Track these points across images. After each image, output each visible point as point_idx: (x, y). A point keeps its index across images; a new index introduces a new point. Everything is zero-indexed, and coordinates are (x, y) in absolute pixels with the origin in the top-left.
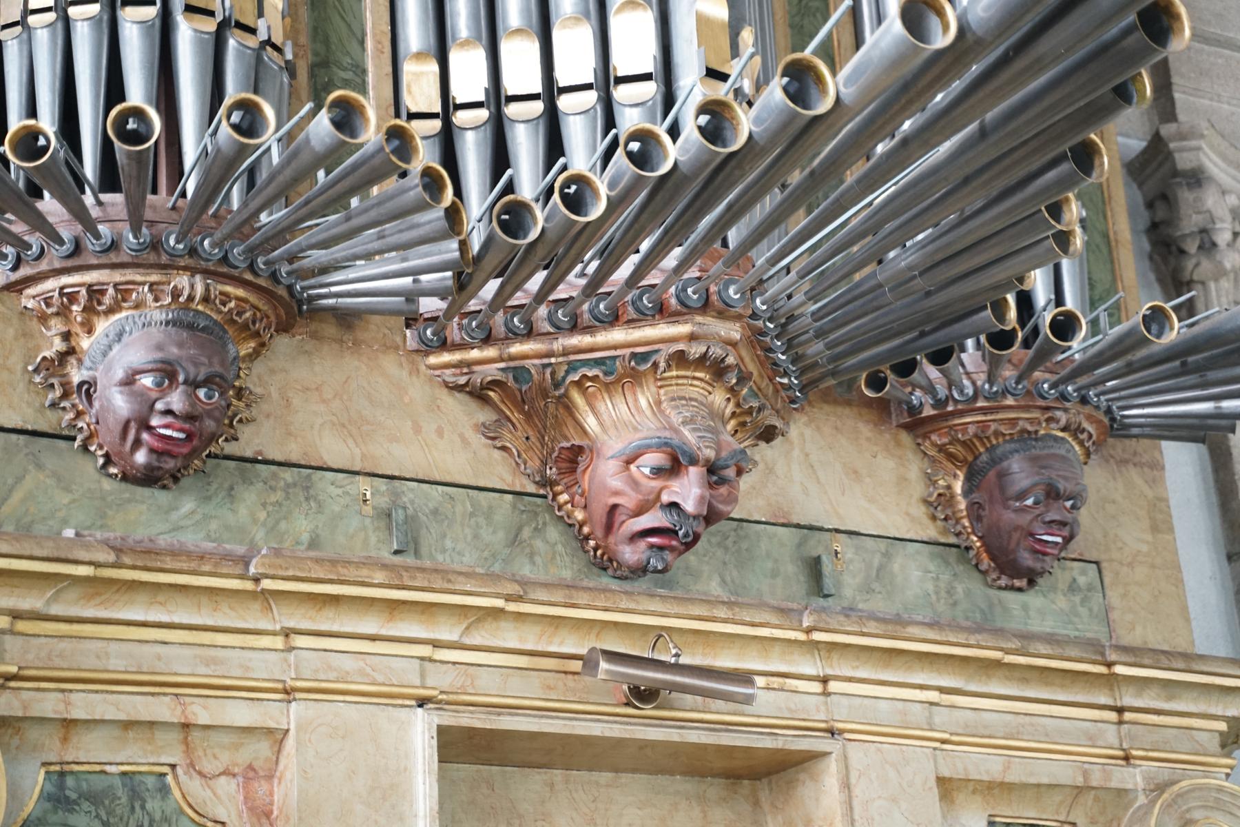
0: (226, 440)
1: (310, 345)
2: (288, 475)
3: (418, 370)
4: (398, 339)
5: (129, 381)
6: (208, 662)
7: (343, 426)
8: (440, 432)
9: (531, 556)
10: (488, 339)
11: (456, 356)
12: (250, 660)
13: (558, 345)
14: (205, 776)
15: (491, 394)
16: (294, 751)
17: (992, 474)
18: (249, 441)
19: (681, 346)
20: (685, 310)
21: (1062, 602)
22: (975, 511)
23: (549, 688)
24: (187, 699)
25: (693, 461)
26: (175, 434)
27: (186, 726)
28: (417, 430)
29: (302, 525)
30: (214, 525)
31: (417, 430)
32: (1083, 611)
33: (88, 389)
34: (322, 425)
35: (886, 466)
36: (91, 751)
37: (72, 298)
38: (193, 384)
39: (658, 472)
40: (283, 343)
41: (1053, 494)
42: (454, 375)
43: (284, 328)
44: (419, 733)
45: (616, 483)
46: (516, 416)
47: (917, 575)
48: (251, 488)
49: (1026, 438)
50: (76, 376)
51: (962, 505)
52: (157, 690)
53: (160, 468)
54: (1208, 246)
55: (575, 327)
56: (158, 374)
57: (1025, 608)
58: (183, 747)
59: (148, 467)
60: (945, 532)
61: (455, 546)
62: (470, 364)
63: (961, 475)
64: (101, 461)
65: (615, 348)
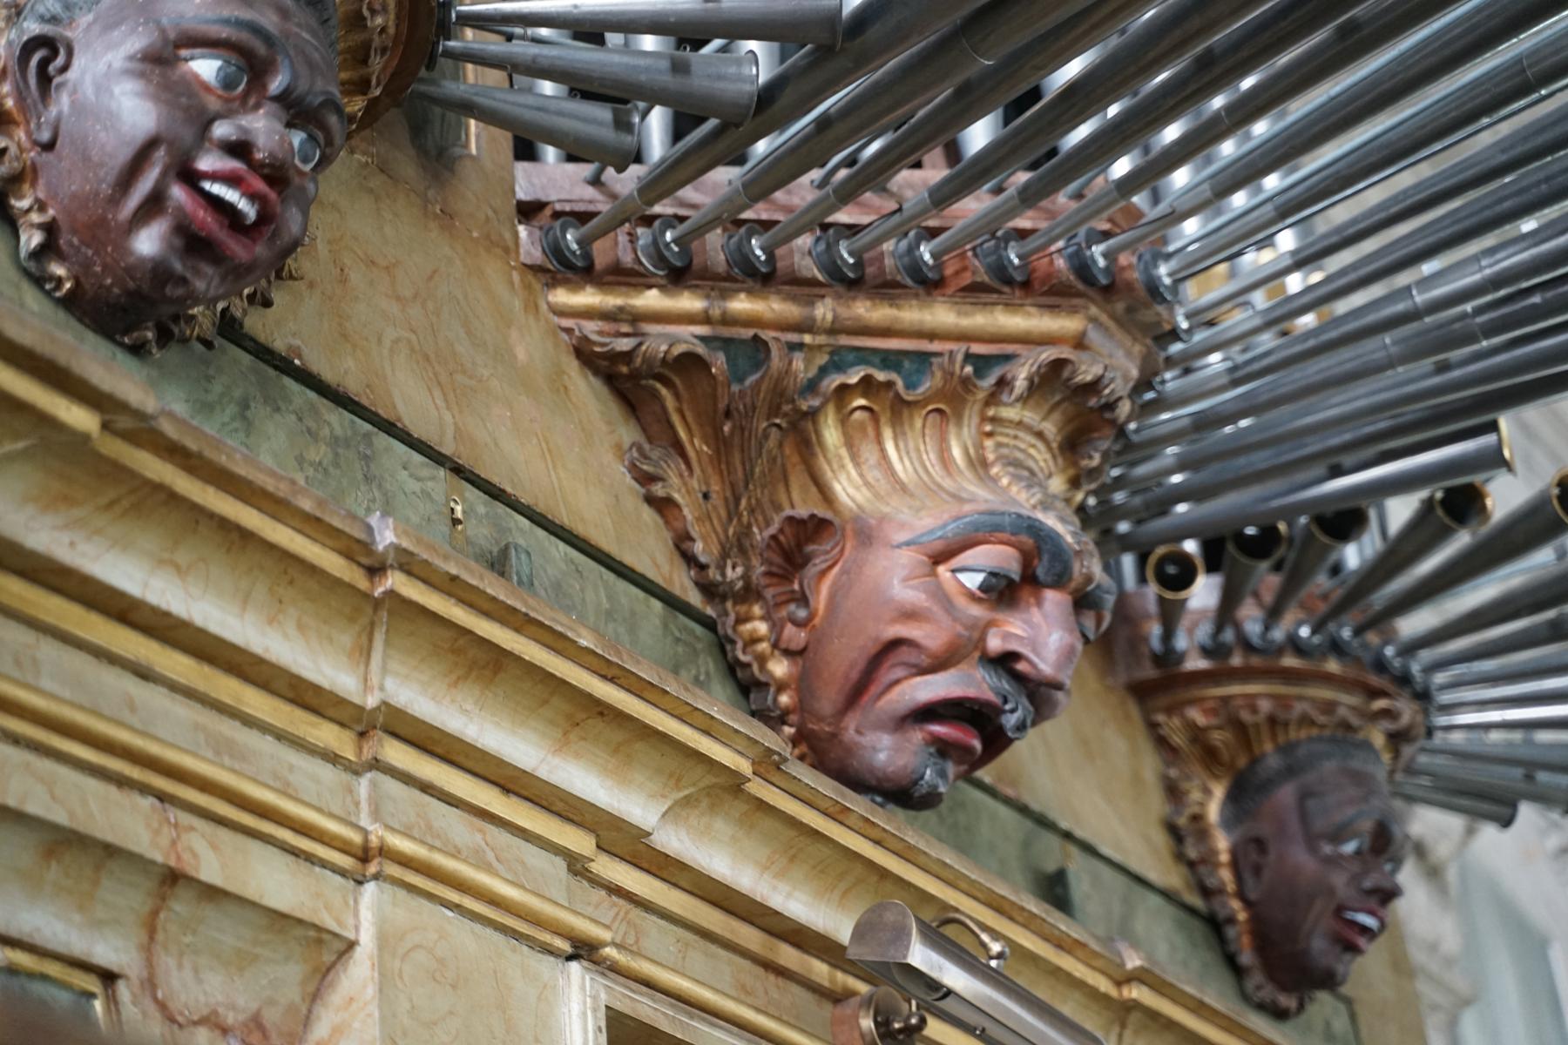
0: (251, 298)
1: (377, 181)
2: (337, 419)
3: (537, 307)
4: (508, 235)
7: (427, 358)
11: (612, 301)
12: (291, 768)
13: (824, 311)
14: (172, 1020)
15: (664, 391)
16: (371, 991)
17: (1286, 794)
18: (287, 323)
19: (1065, 352)
20: (1054, 295)
23: (743, 988)
24: (186, 818)
25: (1059, 582)
26: (243, 205)
27: (173, 878)
34: (396, 341)
42: (600, 333)
45: (907, 593)
46: (697, 446)
48: (277, 416)
51: (1222, 843)
52: (134, 772)
53: (183, 281)
56: (234, 58)
58: (143, 937)
59: (159, 272)
62: (637, 318)
63: (1219, 791)
64: (32, 239)
65: (932, 336)
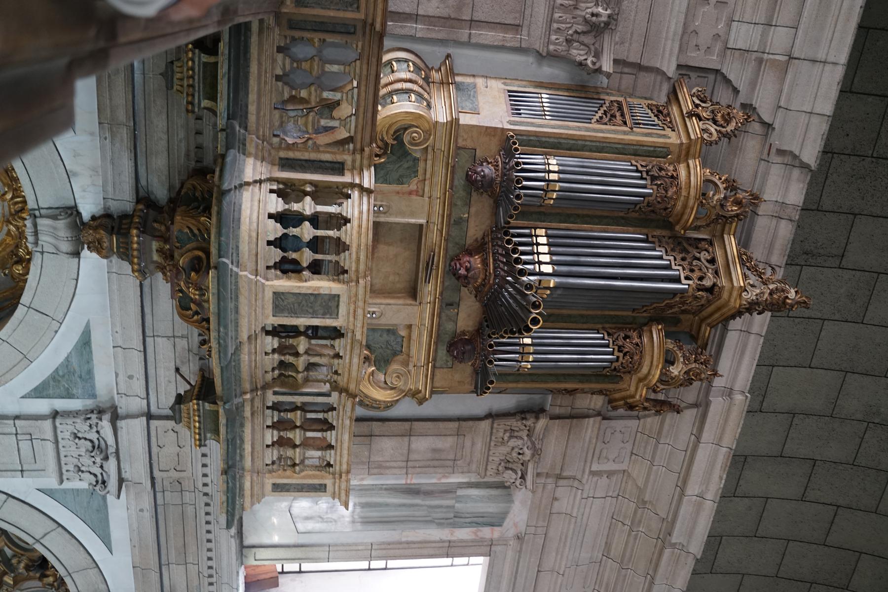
5: (483, 171)
18: (474, 194)
21: (444, 358)
22: (461, 339)
33: (482, 165)
35: (471, 323)
36: (421, 165)
40: (491, 201)
41: (464, 353)
44: (423, 221)
47: (449, 326)
49: (474, 349)
54: (523, 419)
55: (493, 253)
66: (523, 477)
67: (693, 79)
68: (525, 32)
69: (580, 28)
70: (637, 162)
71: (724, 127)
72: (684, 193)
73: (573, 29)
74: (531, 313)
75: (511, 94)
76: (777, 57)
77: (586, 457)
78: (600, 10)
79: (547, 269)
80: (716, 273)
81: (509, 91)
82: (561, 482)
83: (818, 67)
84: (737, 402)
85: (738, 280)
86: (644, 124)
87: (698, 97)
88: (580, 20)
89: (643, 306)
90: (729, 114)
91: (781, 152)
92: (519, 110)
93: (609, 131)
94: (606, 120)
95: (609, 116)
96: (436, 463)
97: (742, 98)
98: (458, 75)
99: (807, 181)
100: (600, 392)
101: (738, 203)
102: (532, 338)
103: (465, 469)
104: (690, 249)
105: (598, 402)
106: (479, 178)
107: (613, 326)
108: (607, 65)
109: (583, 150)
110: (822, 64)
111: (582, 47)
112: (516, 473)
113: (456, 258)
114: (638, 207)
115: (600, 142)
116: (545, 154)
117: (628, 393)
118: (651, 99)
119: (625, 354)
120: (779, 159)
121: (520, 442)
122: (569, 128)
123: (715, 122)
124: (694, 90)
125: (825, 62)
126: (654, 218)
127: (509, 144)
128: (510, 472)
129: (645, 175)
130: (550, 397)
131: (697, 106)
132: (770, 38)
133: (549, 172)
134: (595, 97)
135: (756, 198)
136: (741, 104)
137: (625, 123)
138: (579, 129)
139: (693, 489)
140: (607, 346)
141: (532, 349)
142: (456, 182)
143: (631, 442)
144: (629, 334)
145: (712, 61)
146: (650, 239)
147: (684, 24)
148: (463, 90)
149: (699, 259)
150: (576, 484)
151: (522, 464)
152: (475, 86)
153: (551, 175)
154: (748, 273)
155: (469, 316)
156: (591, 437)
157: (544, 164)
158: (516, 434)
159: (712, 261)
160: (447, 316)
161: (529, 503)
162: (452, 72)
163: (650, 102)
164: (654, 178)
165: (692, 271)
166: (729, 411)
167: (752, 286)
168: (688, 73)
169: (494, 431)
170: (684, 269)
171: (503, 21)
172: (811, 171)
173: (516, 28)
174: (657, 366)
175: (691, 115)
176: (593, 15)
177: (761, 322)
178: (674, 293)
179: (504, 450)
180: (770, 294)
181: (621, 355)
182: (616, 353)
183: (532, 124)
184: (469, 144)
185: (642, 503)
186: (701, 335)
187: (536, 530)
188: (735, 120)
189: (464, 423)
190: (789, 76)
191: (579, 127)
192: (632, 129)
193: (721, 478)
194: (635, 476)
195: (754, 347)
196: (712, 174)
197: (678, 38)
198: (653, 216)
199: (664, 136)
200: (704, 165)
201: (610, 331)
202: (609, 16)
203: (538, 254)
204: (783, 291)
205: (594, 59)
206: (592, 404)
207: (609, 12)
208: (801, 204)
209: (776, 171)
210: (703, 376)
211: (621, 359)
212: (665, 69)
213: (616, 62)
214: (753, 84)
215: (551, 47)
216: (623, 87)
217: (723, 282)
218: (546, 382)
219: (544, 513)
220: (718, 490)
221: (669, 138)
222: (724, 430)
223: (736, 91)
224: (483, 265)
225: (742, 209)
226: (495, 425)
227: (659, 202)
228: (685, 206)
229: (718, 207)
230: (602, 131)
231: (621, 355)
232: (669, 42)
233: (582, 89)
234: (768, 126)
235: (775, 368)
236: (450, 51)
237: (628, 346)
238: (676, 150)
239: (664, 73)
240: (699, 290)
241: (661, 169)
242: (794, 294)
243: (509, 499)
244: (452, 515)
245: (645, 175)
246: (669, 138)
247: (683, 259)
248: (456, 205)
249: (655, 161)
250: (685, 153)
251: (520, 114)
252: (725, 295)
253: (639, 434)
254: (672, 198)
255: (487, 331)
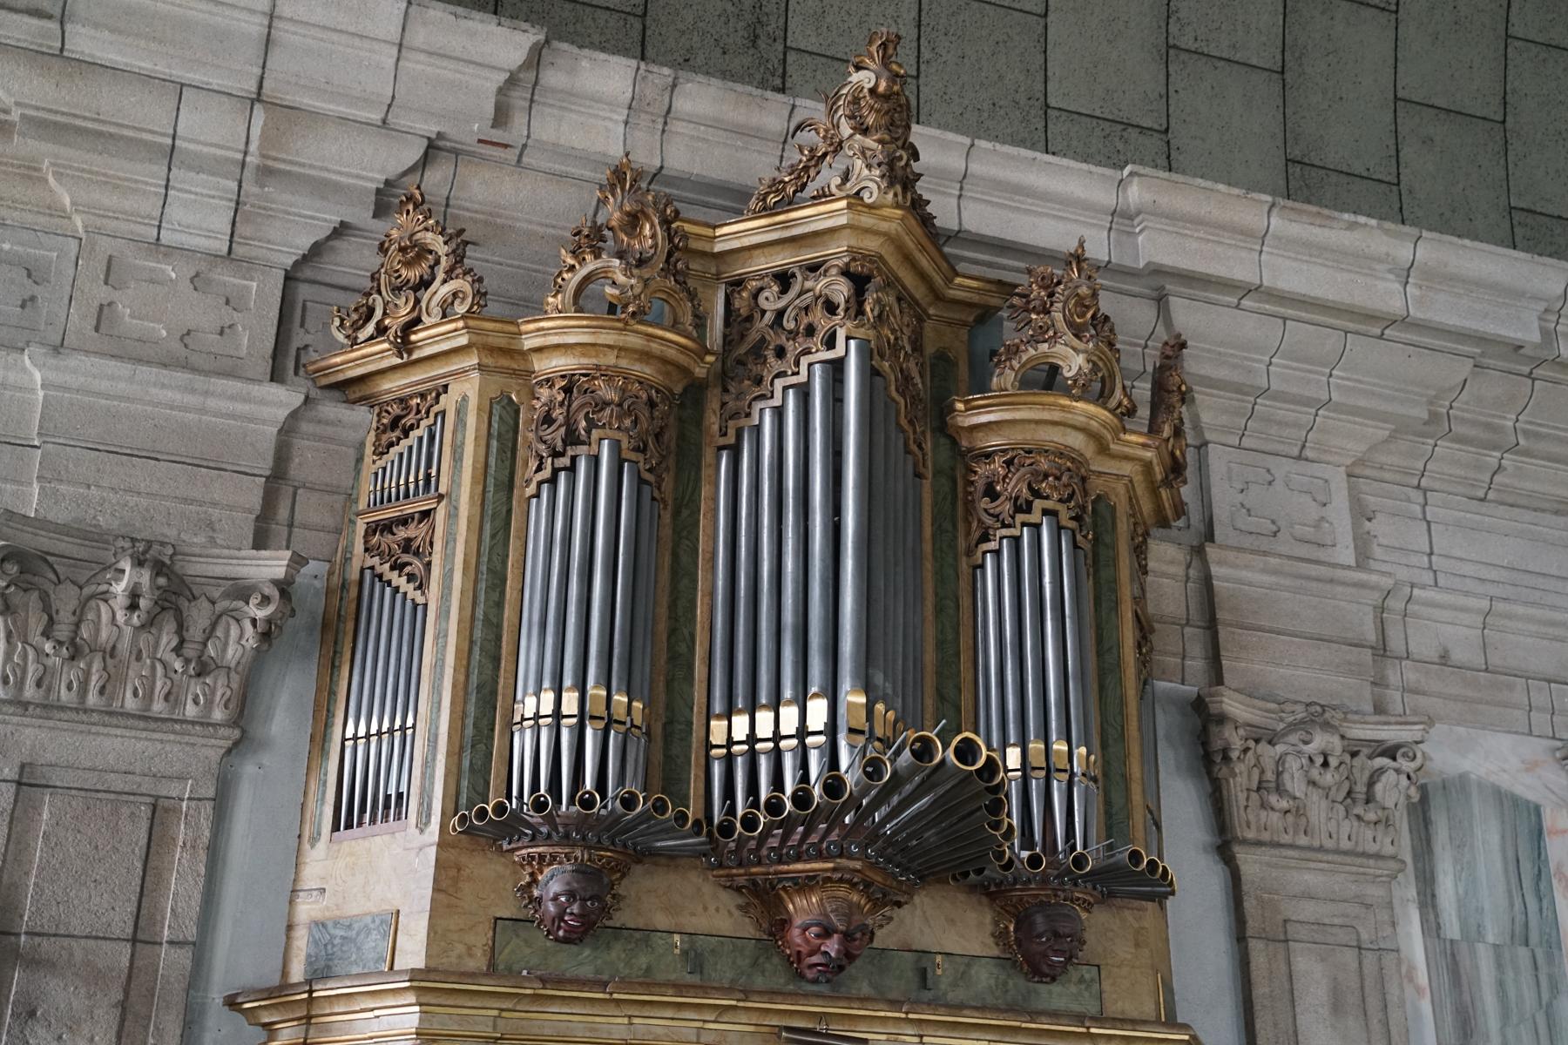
2: (638, 935)
5: (555, 899)
6: (591, 1030)
8: (717, 910)
9: (763, 972)
10: (740, 865)
18: (619, 919)
21: (1073, 989)
22: (1018, 942)
28: (705, 909)
29: (643, 961)
30: (599, 962)
31: (705, 909)
32: (1086, 994)
33: (539, 900)
35: (972, 916)
37: (533, 858)
38: (584, 900)
39: (818, 936)
40: (637, 870)
41: (1057, 935)
43: (639, 862)
45: (798, 940)
47: (984, 977)
49: (1043, 905)
50: (536, 893)
54: (1226, 758)
55: (780, 862)
57: (1050, 992)
60: (1004, 951)
61: (722, 971)
66: (1391, 752)
67: (308, 339)
68: (173, 789)
69: (168, 639)
70: (528, 482)
71: (437, 262)
72: (610, 359)
73: (170, 657)
74: (943, 761)
75: (346, 819)
76: (256, 131)
77: (1318, 580)
78: (120, 588)
79: (818, 713)
80: (813, 268)
81: (336, 827)
82: (1396, 643)
83: (283, 31)
84: (1148, 197)
85: (834, 213)
86: (429, 466)
87: (357, 327)
88: (144, 640)
89: (908, 451)
90: (402, 250)
91: (501, 116)
92: (387, 797)
93: (448, 557)
94: (417, 566)
95: (406, 558)
96: (1373, 1002)
97: (361, 215)
98: (285, 973)
99: (575, 50)
100: (1140, 551)
101: (633, 221)
102: (1005, 744)
103: (1384, 916)
104: (754, 336)
105: (1166, 555)
106: (575, 908)
107: (961, 526)
108: (272, 565)
109: (499, 626)
110: (276, 23)
111: (219, 632)
112: (1381, 771)
113: (794, 965)
114: (647, 476)
115: (476, 582)
116: (509, 725)
117: (1138, 479)
118: (362, 445)
119: (1037, 494)
120: (519, 120)
121: (1293, 764)
122: (439, 664)
123: (425, 284)
124: (340, 337)
125: (271, 17)
126: (676, 430)
127: (483, 824)
128: (1379, 787)
129: (565, 461)
130: (1161, 685)
131: (381, 330)
132: (206, 150)
133: (557, 714)
134: (354, 592)
135: (620, 177)
136: (374, 216)
137: (426, 514)
138: (441, 635)
139: (1387, 296)
140: (1016, 541)
141: (1036, 746)
142: (587, 971)
143: (1270, 461)
144: (981, 485)
145: (263, 292)
146: (731, 440)
147: (165, 366)
148: (330, 957)
149: (780, 314)
150: (1396, 604)
151: (1354, 754)
152: (320, 925)
153: (565, 710)
154: (812, 189)
155: (952, 922)
156: (1264, 571)
157: (537, 729)
158: (1270, 776)
159: (784, 279)
160: (954, 985)
161: (1461, 730)
162: (278, 992)
163: (369, 449)
164: (572, 439)
165: (810, 331)
166: (1171, 217)
167: (846, 178)
168: (293, 353)
169: (1266, 836)
170: (807, 352)
171: (139, 851)
172: (547, 41)
173: (160, 813)
174: (1063, 408)
175: (404, 344)
176: (133, 607)
177: (937, 149)
178: (870, 374)
179: (1318, 809)
180: (865, 131)
181: (1038, 504)
182: (1034, 517)
183: (428, 764)
184: (480, 938)
185: (1437, 424)
186: (975, 298)
187: (1541, 710)
188: (420, 228)
189: (1250, 923)
190: (306, 101)
191: (436, 638)
192: (441, 497)
193: (1352, 226)
194: (1364, 448)
195: (1000, 162)
196: (559, 289)
197: (199, 381)
198: (670, 436)
199: (460, 412)
200: (536, 309)
201: (976, 535)
202: (139, 563)
203: (777, 737)
204: (856, 101)
205: (253, 601)
206: (1172, 569)
207: (126, 565)
208: (634, 63)
209: (551, 128)
210: (1084, 290)
211: (1049, 504)
212: (282, 414)
213: (261, 541)
214: (323, 188)
215: (218, 715)
216: (329, 521)
217: (836, 250)
218: (1122, 703)
219: (1490, 687)
220: (1387, 232)
221: (465, 398)
222: (1222, 227)
223: (342, 230)
224: (811, 889)
225: (650, 211)
226: (1250, 835)
227: (635, 422)
228: (645, 356)
229: (646, 273)
230: (448, 576)
231: (1038, 504)
232: (212, 403)
233: (333, 627)
234: (433, 149)
235: (1052, 102)
236: (216, 997)
237: (1015, 486)
238: (497, 384)
239: (294, 415)
240: (860, 312)
241: (548, 420)
242: (862, 74)
243: (1459, 786)
244: (1523, 952)
245: (565, 461)
246: (465, 398)
247: (780, 353)
248: (648, 970)
249: (526, 434)
250: (504, 358)
251: (400, 796)
252: (872, 244)
253: (1246, 442)
254: (623, 390)
255: (993, 871)
